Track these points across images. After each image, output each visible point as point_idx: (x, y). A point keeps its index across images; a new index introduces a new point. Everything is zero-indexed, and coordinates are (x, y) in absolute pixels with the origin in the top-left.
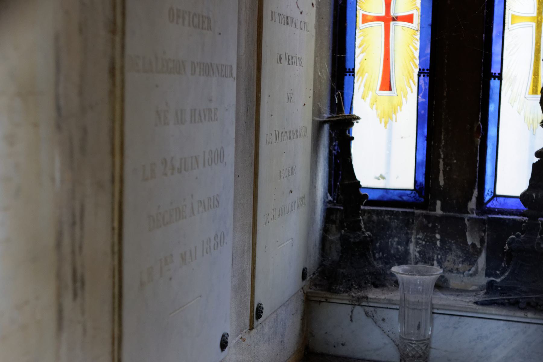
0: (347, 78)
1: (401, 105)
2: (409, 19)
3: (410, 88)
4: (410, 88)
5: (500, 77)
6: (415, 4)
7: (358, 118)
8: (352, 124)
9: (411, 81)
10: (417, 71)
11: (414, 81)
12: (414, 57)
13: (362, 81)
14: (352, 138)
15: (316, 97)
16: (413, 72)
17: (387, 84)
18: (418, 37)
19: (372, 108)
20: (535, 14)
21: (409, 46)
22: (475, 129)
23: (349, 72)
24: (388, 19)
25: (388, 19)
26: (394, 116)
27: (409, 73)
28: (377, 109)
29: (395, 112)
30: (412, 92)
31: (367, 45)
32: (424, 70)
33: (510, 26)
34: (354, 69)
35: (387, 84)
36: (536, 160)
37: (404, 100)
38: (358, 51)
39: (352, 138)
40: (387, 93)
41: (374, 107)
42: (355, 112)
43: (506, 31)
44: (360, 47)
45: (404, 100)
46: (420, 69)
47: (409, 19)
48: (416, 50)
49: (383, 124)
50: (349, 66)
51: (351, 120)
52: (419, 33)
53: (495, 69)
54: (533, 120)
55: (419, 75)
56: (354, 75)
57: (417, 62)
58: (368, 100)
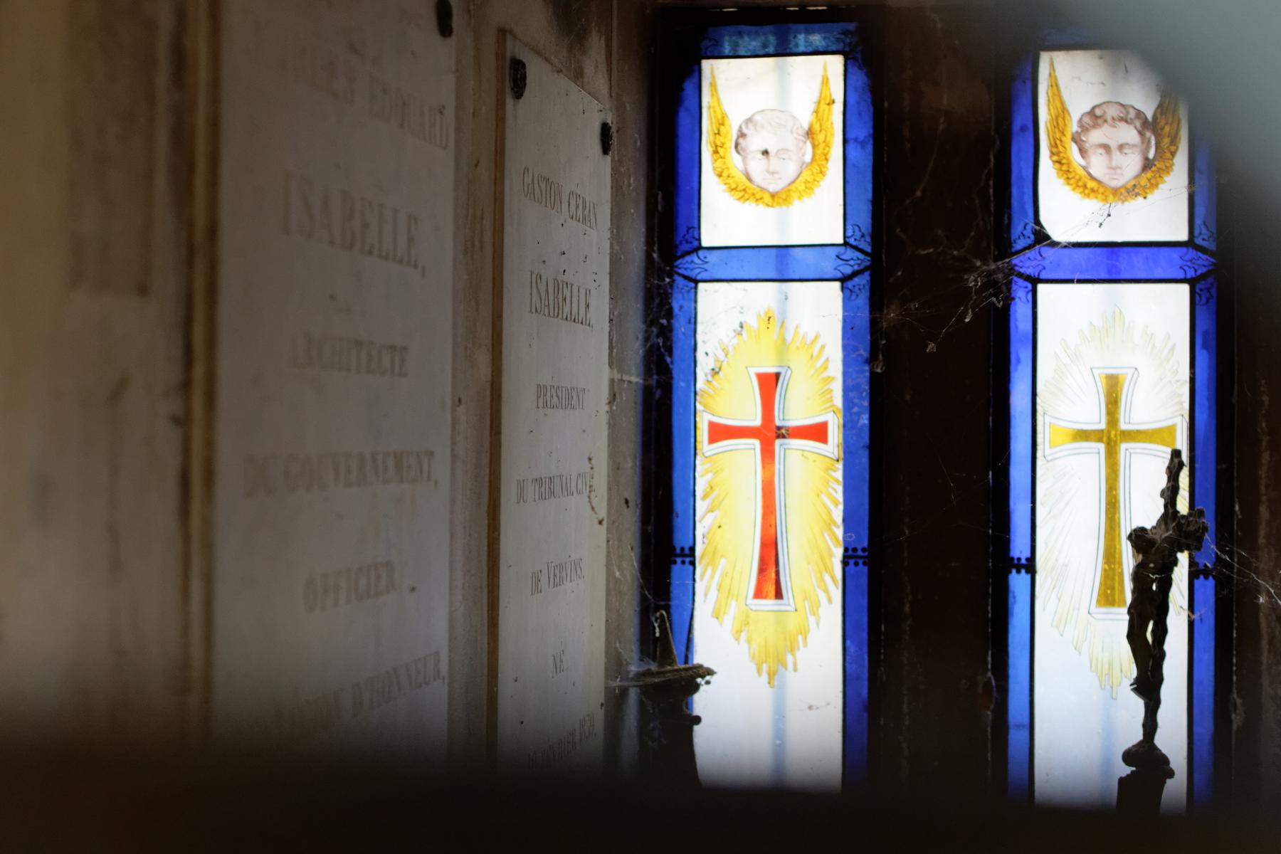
0: (677, 570)
1: (804, 632)
2: (817, 432)
3: (826, 591)
4: (826, 591)
5: (1030, 567)
6: (831, 399)
7: (710, 672)
8: (696, 688)
9: (827, 577)
10: (839, 553)
11: (833, 578)
12: (833, 522)
13: (712, 576)
14: (697, 720)
15: (613, 631)
16: (831, 555)
17: (770, 577)
18: (839, 475)
19: (737, 639)
20: (1103, 426)
21: (816, 497)
22: (980, 690)
23: (683, 555)
24: (770, 434)
25: (770, 434)
26: (790, 659)
27: (822, 559)
28: (749, 641)
29: (793, 649)
30: (830, 601)
31: (721, 492)
32: (855, 550)
33: (1048, 452)
34: (692, 549)
35: (770, 577)
36: (1126, 770)
37: (812, 619)
38: (701, 506)
39: (697, 720)
40: (769, 603)
41: (743, 636)
42: (701, 657)
43: (1039, 463)
44: (704, 497)
45: (812, 619)
46: (846, 550)
47: (817, 432)
48: (836, 504)
49: (765, 677)
50: (680, 541)
51: (692, 678)
52: (840, 466)
53: (1019, 549)
54: (1110, 664)
55: (845, 563)
56: (693, 563)
57: (840, 532)
58: (728, 620)
